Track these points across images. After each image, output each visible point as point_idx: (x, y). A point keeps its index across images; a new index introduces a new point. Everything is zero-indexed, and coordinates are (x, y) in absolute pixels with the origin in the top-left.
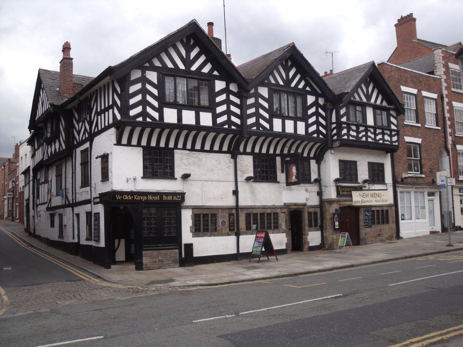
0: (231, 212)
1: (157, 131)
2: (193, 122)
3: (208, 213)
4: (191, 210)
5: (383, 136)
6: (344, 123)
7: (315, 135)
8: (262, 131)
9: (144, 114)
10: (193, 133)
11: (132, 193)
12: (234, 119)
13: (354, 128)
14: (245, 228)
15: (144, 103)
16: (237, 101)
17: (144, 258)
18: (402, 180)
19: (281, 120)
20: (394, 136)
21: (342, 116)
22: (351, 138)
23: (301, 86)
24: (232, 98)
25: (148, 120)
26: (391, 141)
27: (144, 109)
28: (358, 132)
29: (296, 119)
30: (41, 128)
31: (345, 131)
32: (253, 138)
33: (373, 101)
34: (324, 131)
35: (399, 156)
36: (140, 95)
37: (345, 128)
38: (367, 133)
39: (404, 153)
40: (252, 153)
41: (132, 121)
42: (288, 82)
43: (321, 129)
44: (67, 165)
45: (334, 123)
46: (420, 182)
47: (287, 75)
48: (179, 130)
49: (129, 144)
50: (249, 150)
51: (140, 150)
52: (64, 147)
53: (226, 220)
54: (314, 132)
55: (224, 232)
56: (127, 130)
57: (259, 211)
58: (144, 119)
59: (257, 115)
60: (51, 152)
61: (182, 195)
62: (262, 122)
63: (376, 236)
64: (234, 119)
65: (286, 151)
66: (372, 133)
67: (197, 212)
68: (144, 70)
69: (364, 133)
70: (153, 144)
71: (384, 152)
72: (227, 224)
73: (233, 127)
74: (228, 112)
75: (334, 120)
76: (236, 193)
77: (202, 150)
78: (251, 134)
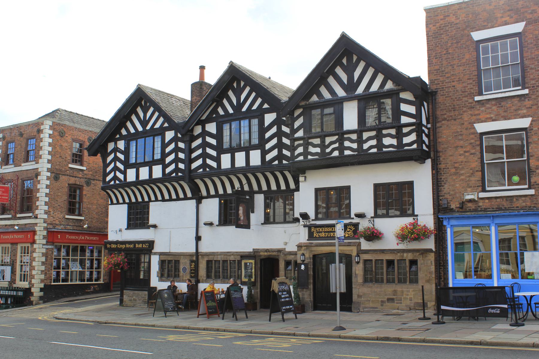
0: (192, 259)
8: (210, 172)
9: (115, 178)
11: (117, 242)
14: (205, 275)
17: (124, 296)
18: (463, 205)
22: (310, 157)
25: (117, 182)
31: (300, 150)
38: (341, 144)
39: (472, 156)
40: (217, 195)
41: (108, 185)
46: (518, 205)
47: (238, 99)
53: (188, 267)
55: (184, 279)
57: (219, 258)
61: (151, 244)
63: (382, 302)
67: (164, 258)
68: (116, 141)
72: (188, 271)
74: (177, 160)
76: (198, 238)
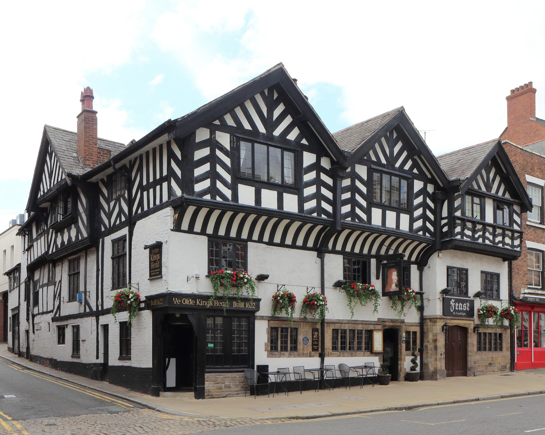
0: (315, 327)
1: (228, 215)
2: (273, 206)
3: (287, 326)
4: (266, 322)
5: (503, 238)
6: (459, 218)
7: (421, 233)
10: (274, 220)
12: (324, 205)
13: (469, 225)
15: (213, 175)
16: (329, 181)
17: (206, 383)
19: (381, 210)
20: (516, 239)
21: (456, 210)
22: (465, 238)
23: (407, 167)
24: (324, 177)
25: (218, 199)
26: (513, 246)
27: (213, 184)
28: (474, 231)
29: (399, 210)
30: (45, 209)
31: (458, 229)
32: (346, 232)
33: (493, 191)
34: (432, 229)
35: (518, 265)
36: (208, 164)
37: (459, 225)
38: (484, 233)
39: (525, 262)
40: (343, 252)
41: (198, 198)
42: (392, 160)
43: (428, 225)
44: (88, 259)
45: (444, 218)
48: (256, 215)
49: (191, 230)
50: (339, 247)
51: (205, 239)
52: (85, 235)
54: (419, 230)
56: (191, 210)
58: (213, 197)
59: (352, 201)
60: (63, 242)
62: (358, 211)
64: (324, 205)
65: (383, 252)
66: (490, 234)
69: (480, 233)
70: (222, 232)
71: (500, 260)
73: (323, 216)
74: (318, 196)
75: (445, 213)
77: (282, 244)
78: (345, 226)
